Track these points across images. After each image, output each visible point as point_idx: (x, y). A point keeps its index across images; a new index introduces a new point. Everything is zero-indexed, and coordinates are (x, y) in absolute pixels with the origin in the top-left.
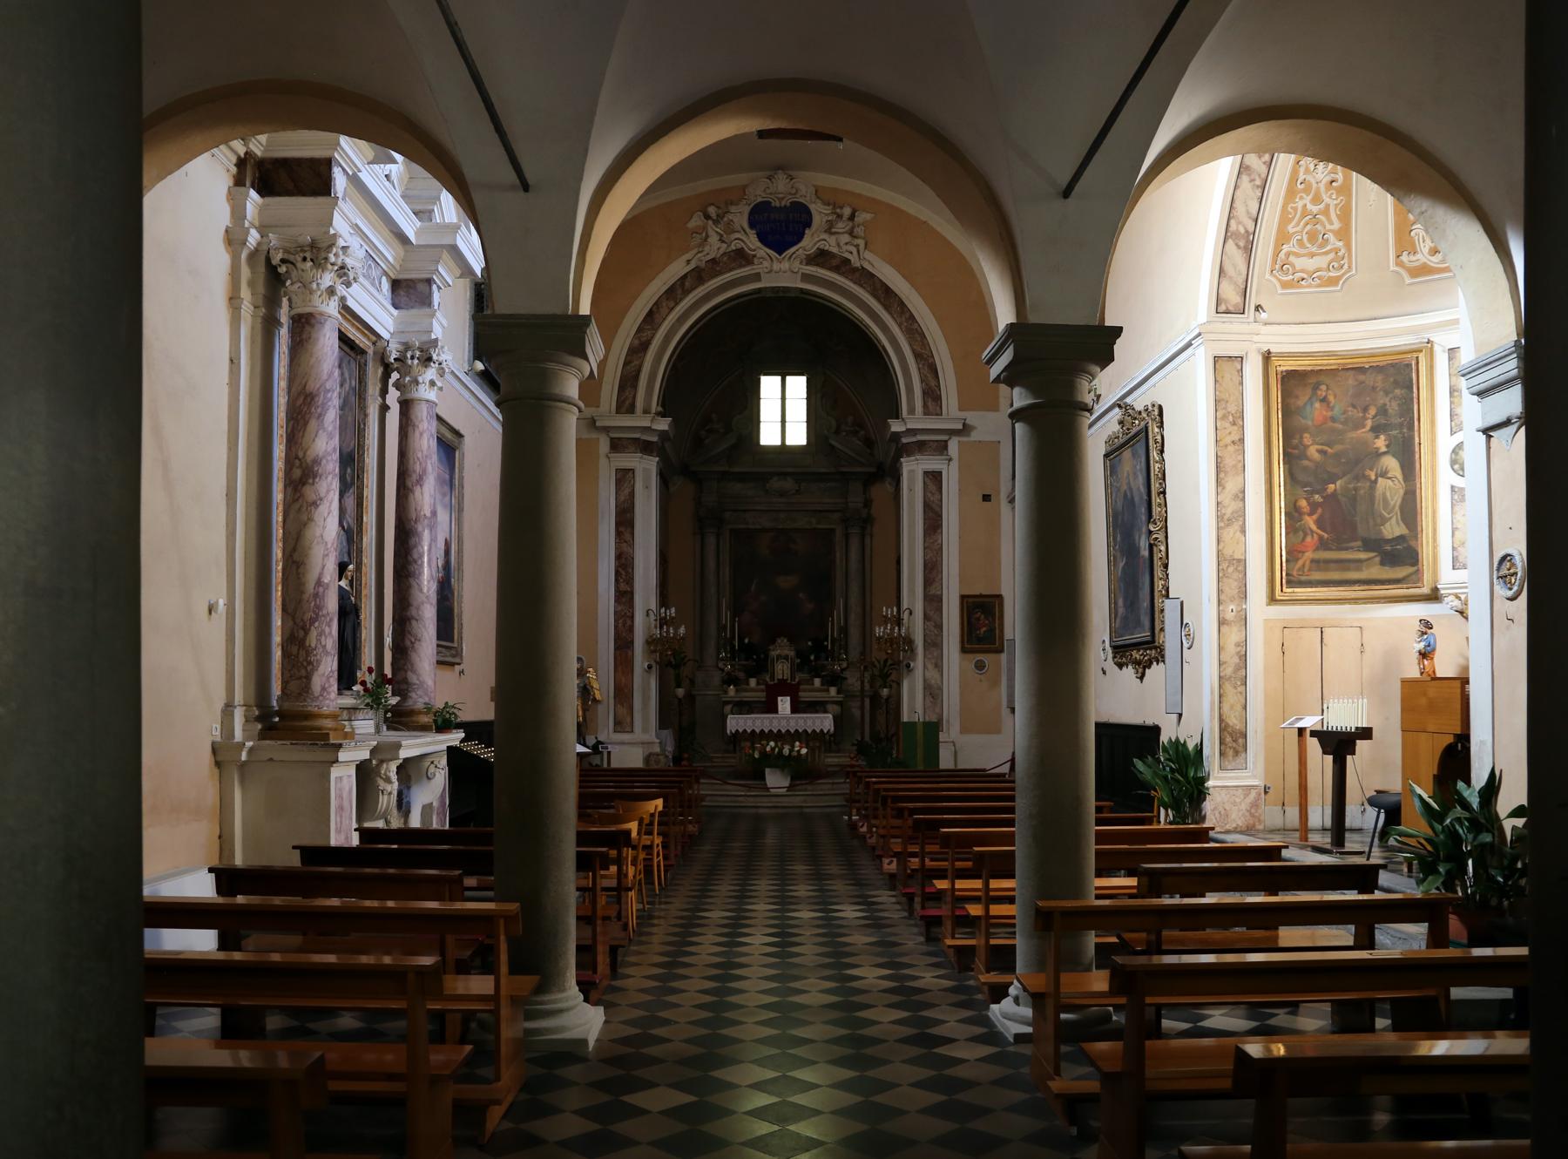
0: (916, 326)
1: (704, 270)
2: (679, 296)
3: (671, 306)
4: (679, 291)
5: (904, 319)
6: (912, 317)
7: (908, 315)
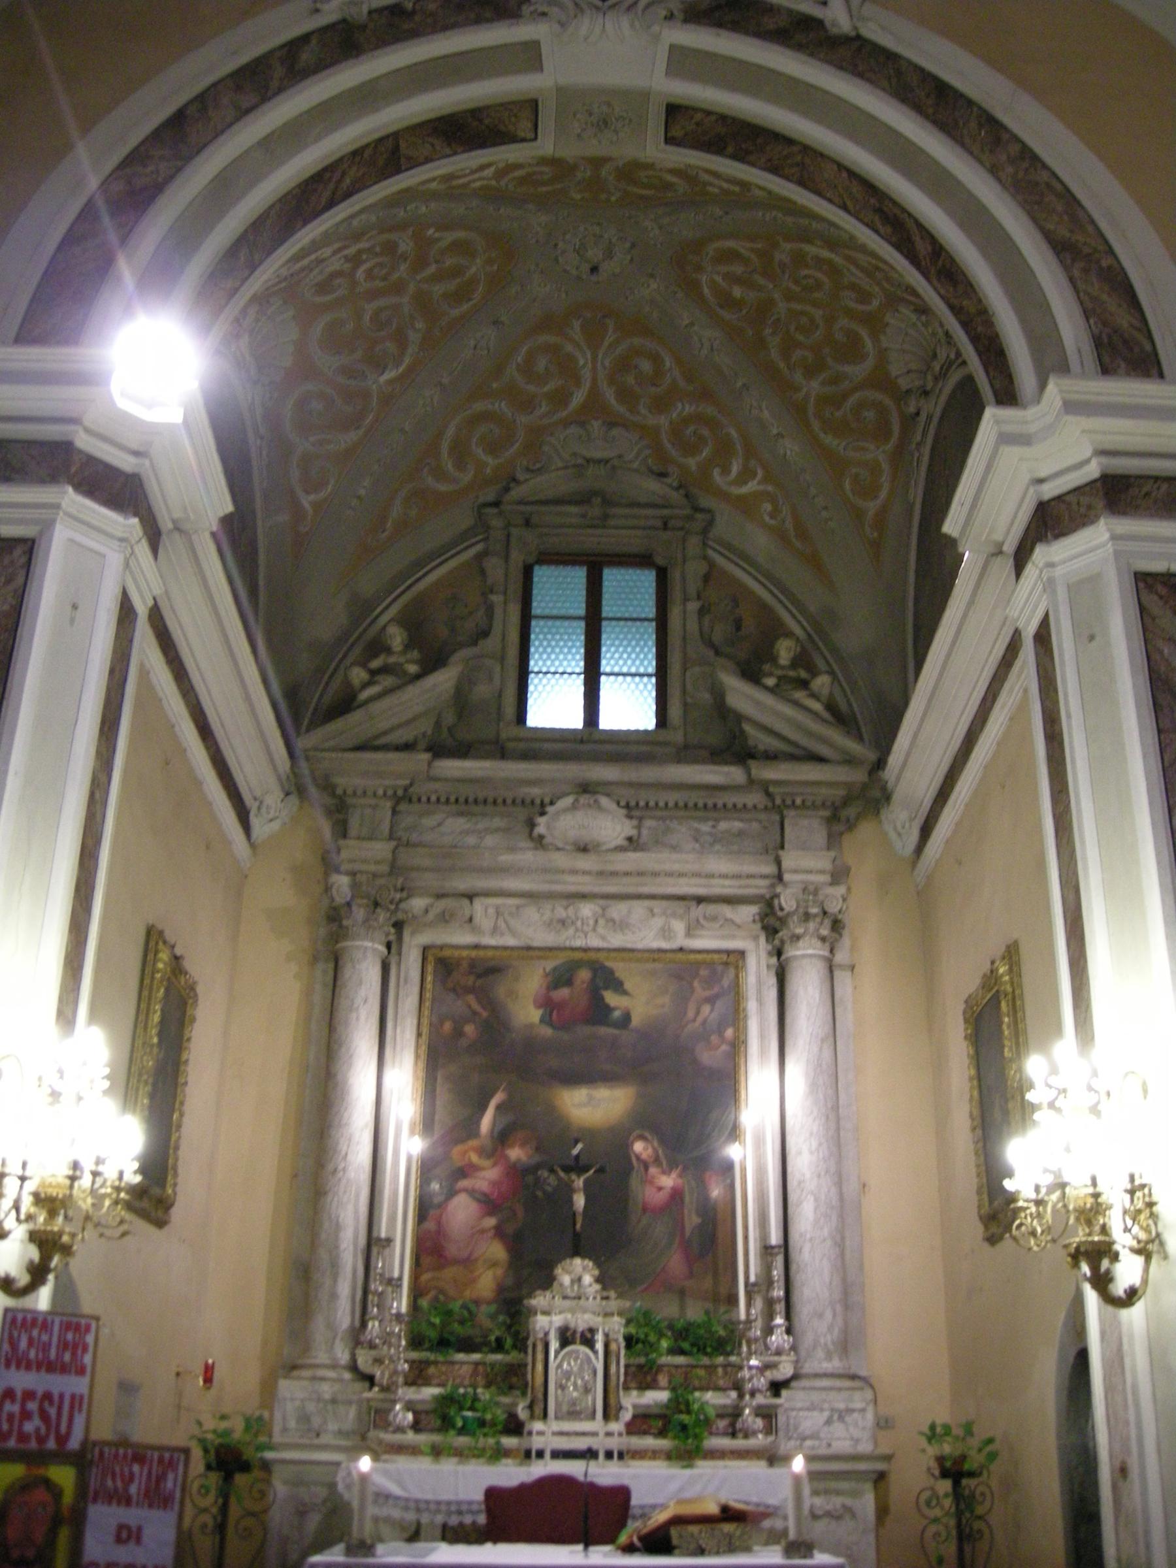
0: (1045, 176)
1: (363, 27)
2: (274, 84)
3: (245, 105)
4: (279, 71)
5: (1004, 158)
6: (1028, 156)
7: (1014, 149)
